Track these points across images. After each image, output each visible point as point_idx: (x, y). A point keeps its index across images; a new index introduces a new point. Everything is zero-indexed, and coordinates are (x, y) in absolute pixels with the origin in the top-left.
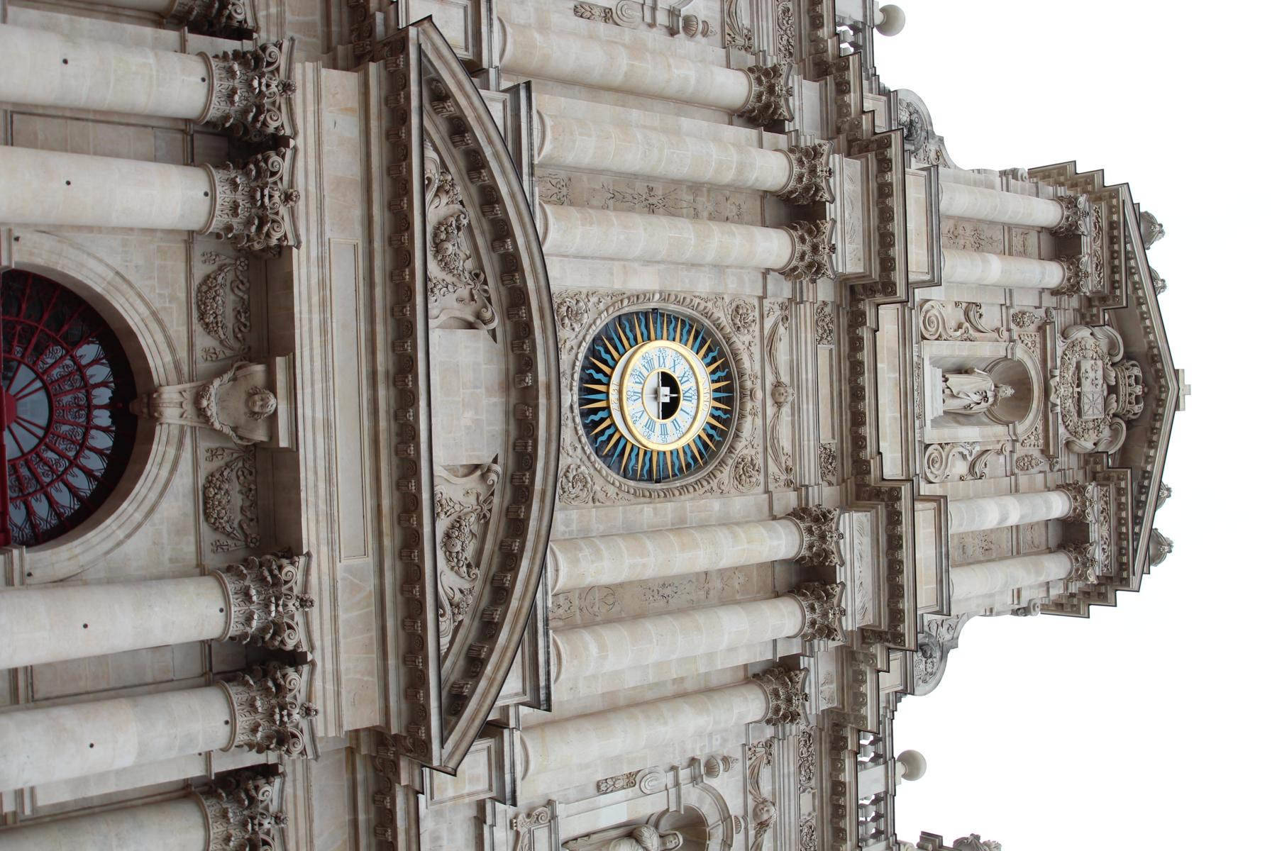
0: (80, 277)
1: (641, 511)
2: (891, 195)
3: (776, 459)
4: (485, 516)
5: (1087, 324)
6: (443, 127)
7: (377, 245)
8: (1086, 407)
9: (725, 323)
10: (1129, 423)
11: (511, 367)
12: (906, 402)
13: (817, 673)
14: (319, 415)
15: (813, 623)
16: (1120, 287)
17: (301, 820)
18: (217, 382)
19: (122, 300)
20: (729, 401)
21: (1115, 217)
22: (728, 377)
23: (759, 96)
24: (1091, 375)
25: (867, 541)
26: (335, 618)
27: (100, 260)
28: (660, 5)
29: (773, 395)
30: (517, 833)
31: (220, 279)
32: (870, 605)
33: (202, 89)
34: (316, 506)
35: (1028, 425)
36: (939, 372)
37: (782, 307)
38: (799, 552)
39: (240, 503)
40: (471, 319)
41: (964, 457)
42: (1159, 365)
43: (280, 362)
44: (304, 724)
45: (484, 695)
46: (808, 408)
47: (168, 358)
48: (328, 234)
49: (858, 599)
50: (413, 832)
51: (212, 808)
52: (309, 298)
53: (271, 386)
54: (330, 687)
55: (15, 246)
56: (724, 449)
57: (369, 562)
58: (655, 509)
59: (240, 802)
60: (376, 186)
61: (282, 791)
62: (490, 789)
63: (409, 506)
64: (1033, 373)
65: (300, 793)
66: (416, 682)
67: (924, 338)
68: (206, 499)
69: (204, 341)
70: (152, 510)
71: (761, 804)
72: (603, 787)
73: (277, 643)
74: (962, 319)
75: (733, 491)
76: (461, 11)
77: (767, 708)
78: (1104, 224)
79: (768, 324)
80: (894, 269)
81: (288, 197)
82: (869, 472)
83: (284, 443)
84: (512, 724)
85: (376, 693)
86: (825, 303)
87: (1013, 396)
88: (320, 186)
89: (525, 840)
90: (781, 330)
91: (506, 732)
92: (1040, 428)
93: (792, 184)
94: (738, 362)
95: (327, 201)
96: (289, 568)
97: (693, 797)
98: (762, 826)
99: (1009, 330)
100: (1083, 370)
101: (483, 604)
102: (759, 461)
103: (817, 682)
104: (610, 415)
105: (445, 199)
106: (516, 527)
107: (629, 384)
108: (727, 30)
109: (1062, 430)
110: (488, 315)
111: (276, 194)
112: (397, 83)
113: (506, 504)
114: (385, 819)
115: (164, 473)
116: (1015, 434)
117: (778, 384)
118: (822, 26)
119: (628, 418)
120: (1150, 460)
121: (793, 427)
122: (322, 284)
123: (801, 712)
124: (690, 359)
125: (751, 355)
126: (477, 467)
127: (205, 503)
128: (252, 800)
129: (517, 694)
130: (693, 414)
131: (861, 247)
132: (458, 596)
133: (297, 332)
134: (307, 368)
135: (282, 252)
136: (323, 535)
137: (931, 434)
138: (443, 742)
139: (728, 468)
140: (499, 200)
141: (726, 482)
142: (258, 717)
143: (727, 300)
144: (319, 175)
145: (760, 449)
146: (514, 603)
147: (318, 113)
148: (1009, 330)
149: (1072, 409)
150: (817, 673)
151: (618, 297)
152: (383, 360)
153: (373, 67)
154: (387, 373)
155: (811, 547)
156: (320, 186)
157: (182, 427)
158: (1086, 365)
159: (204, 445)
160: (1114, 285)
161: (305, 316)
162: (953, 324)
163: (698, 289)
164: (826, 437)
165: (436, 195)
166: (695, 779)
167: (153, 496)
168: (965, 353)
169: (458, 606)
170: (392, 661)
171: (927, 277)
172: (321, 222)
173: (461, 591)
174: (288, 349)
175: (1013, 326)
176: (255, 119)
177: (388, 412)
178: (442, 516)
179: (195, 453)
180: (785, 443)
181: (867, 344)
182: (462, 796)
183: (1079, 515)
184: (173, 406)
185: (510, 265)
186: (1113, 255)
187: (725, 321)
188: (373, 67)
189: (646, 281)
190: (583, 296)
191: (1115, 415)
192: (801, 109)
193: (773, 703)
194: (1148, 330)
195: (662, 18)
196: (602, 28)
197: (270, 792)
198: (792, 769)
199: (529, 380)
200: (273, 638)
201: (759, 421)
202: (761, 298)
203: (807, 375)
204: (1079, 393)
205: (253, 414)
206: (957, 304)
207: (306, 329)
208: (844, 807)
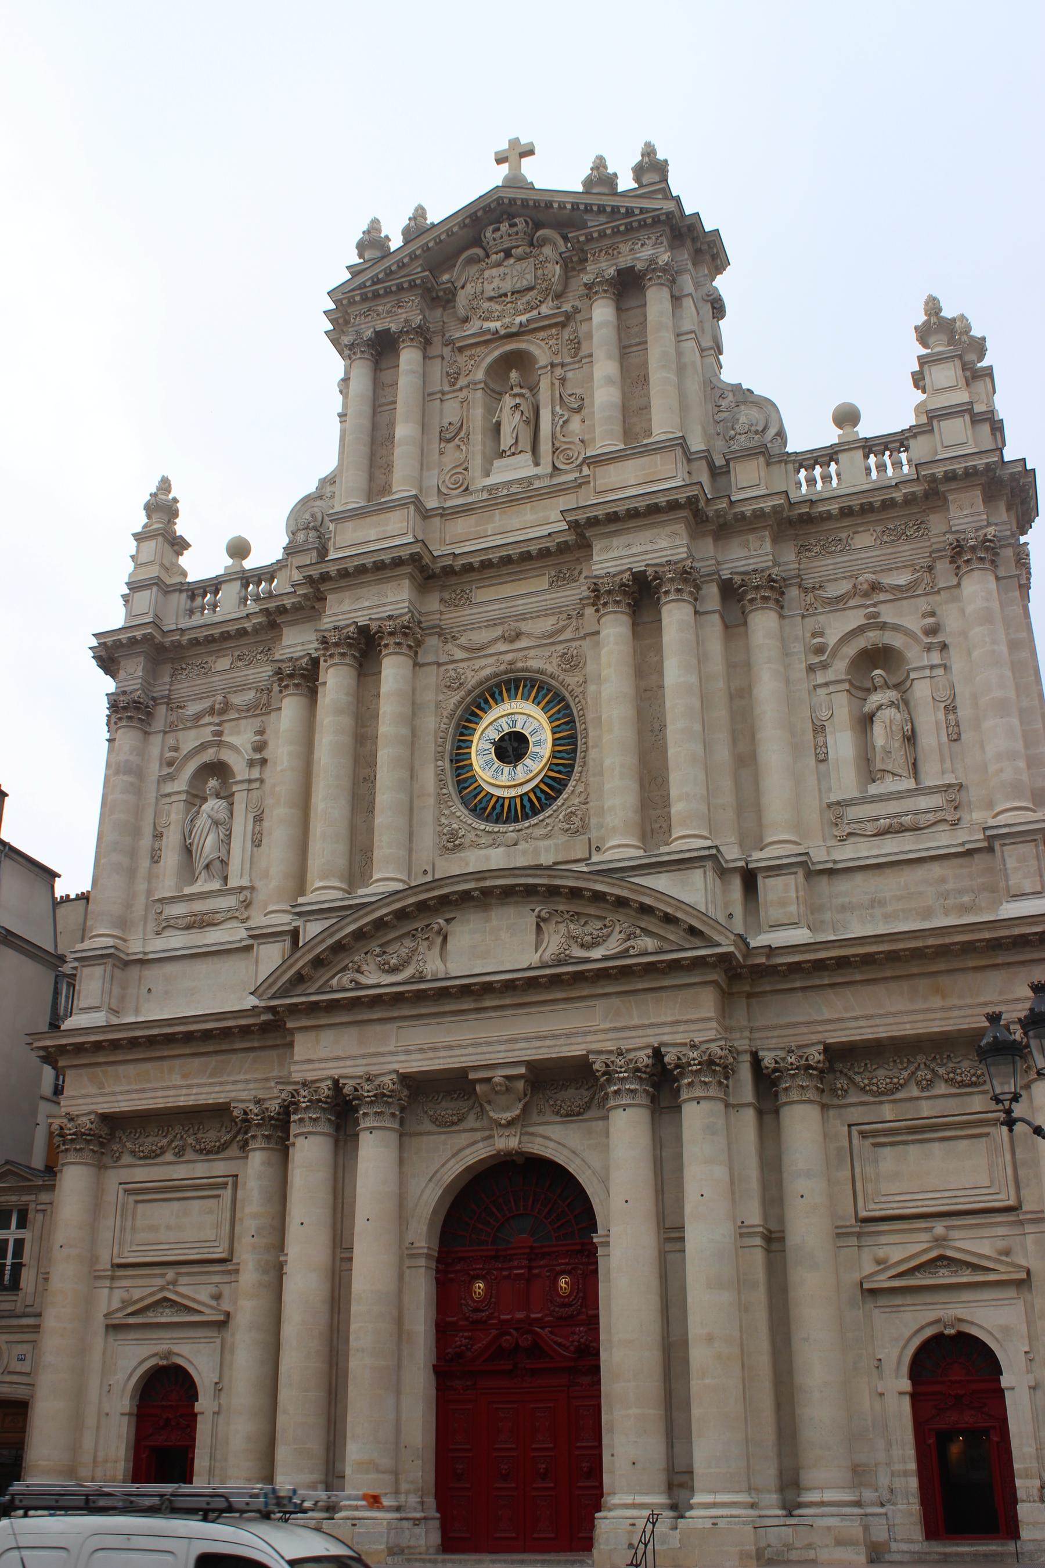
0: (433, 1204)
1: (594, 760)
2: (346, 569)
3: (561, 631)
4: (572, 916)
5: (454, 295)
6: (321, 971)
7: (395, 1014)
8: (525, 283)
9: (458, 698)
10: (538, 225)
11: (472, 904)
12: (518, 500)
13: (738, 559)
14: (503, 1047)
15: (678, 590)
16: (414, 280)
17: (797, 1031)
18: (492, 1114)
19: (446, 1176)
20: (517, 681)
21: (358, 298)
22: (498, 685)
23: (296, 685)
24: (496, 282)
25: (616, 541)
26: (635, 1027)
27: (423, 1191)
28: (247, 777)
29: (512, 641)
30: (850, 834)
31: (431, 1113)
32: (669, 529)
33: (312, 1139)
34: (561, 1045)
35: (540, 350)
36: (497, 463)
38: (622, 612)
39: (573, 1091)
40: (440, 940)
41: (565, 422)
42: (479, 214)
43: (472, 1076)
44: (703, 1047)
45: (687, 913)
46: (522, 605)
47: (481, 1145)
48: (392, 1049)
49: (660, 547)
50: (802, 948)
51: (783, 1099)
52: (431, 1059)
53: (489, 1080)
54: (681, 1028)
55: (416, 1245)
56: (553, 682)
57: (601, 1004)
58: (593, 747)
59: (779, 1078)
60: (360, 1018)
61: (769, 1049)
62: (795, 873)
63: (555, 981)
64: (496, 353)
65: (776, 1033)
66: (675, 966)
67: (467, 489)
68: (568, 1115)
69: (471, 1122)
70: (574, 1152)
71: (855, 592)
72: (822, 757)
73: (648, 1070)
74: (452, 444)
75: (583, 672)
76: (261, 947)
77: (763, 608)
78: (367, 305)
79: (459, 654)
80: (400, 556)
81: (368, 1080)
82: (566, 542)
83: (522, 1070)
84: (742, 864)
85: (691, 991)
86: (441, 600)
87: (517, 369)
88: (363, 1056)
89: (855, 828)
90: (463, 640)
91: (750, 866)
92: (542, 334)
93: (348, 660)
94: (487, 679)
95: (371, 1050)
96: (596, 1067)
97: (840, 667)
98: (875, 587)
99: (461, 389)
100: (492, 294)
101: (633, 913)
102: (560, 648)
103: (747, 558)
104: (526, 793)
105: (365, 968)
106: (575, 893)
107: (504, 779)
108: (258, 712)
109: (545, 310)
110: (436, 927)
111: (367, 1088)
112: (293, 1010)
113: (564, 900)
114: (795, 968)
115: (552, 1144)
116: (546, 367)
117: (503, 638)
118: (244, 628)
119: (528, 777)
120: (562, 206)
121: (536, 617)
122: (421, 1051)
123: (768, 572)
124: (484, 726)
125: (482, 668)
126: (538, 925)
127: (571, 1116)
128: (775, 1070)
129: (705, 873)
130: (525, 717)
131: (389, 585)
132: (622, 936)
133: (452, 1066)
134: (473, 1058)
135: (405, 1079)
136: (579, 1040)
137: (545, 468)
138: (720, 945)
139: (567, 678)
140: (360, 929)
141: (576, 679)
142: (697, 1080)
143: (441, 697)
144: (357, 1057)
145: (553, 648)
146: (625, 893)
147: (320, 1061)
148: (461, 389)
149: (524, 300)
150: (738, 559)
151: (441, 799)
153: (289, 1025)
154: (475, 1001)
155: (617, 602)
156: (363, 1056)
157: (521, 1134)
158: (489, 290)
159: (535, 1118)
160: (413, 286)
161: (442, 1061)
162: (457, 454)
163: (433, 725)
164: (543, 583)
165: (362, 973)
166: (824, 666)
167: (566, 1152)
168: (479, 437)
169: (630, 935)
170: (666, 983)
171: (412, 508)
172: (383, 1054)
173: (620, 932)
174: (463, 1072)
175: (458, 387)
176: (326, 1103)
177: (500, 999)
178: (567, 952)
179: (540, 1124)
180: (547, 625)
181: (466, 560)
182: (797, 897)
183: (611, 284)
184: (508, 1142)
185: (402, 915)
186: (388, 292)
187: (454, 700)
188: (290, 1025)
189: (428, 777)
190: (439, 829)
191: (531, 244)
192: (302, 644)
193: (759, 603)
194: (450, 233)
195: (255, 773)
196: (265, 824)
197: (768, 1059)
198: (829, 561)
199: (476, 894)
200: (645, 1072)
201: (532, 653)
202: (439, 665)
203: (495, 610)
204: (513, 293)
205: (508, 1090)
206: (441, 453)
207: (449, 1060)
208: (861, 504)
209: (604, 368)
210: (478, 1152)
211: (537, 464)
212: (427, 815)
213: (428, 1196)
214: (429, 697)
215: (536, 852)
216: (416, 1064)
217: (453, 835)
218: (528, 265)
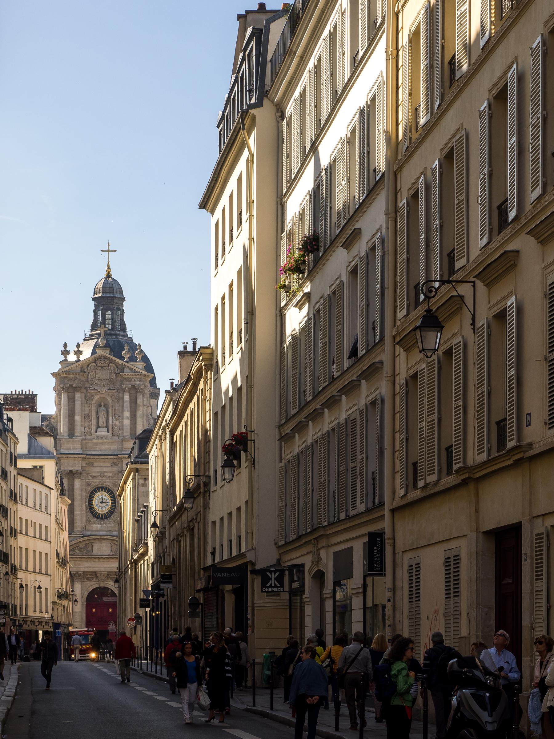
3: (114, 477)
5: (88, 376)
37: (87, 474)
46: (105, 469)
69: (94, 580)
79: (90, 478)
152: (97, 560)
174: (95, 572)
180: (111, 475)
184: (102, 585)
187: (89, 489)
203: (98, 469)
209: (127, 414)
210: (97, 586)
211: (108, 432)
212: (84, 515)
213: (86, 593)
214: (84, 487)
215: (108, 527)
216: (86, 570)
217: (90, 521)
218: (107, 372)
